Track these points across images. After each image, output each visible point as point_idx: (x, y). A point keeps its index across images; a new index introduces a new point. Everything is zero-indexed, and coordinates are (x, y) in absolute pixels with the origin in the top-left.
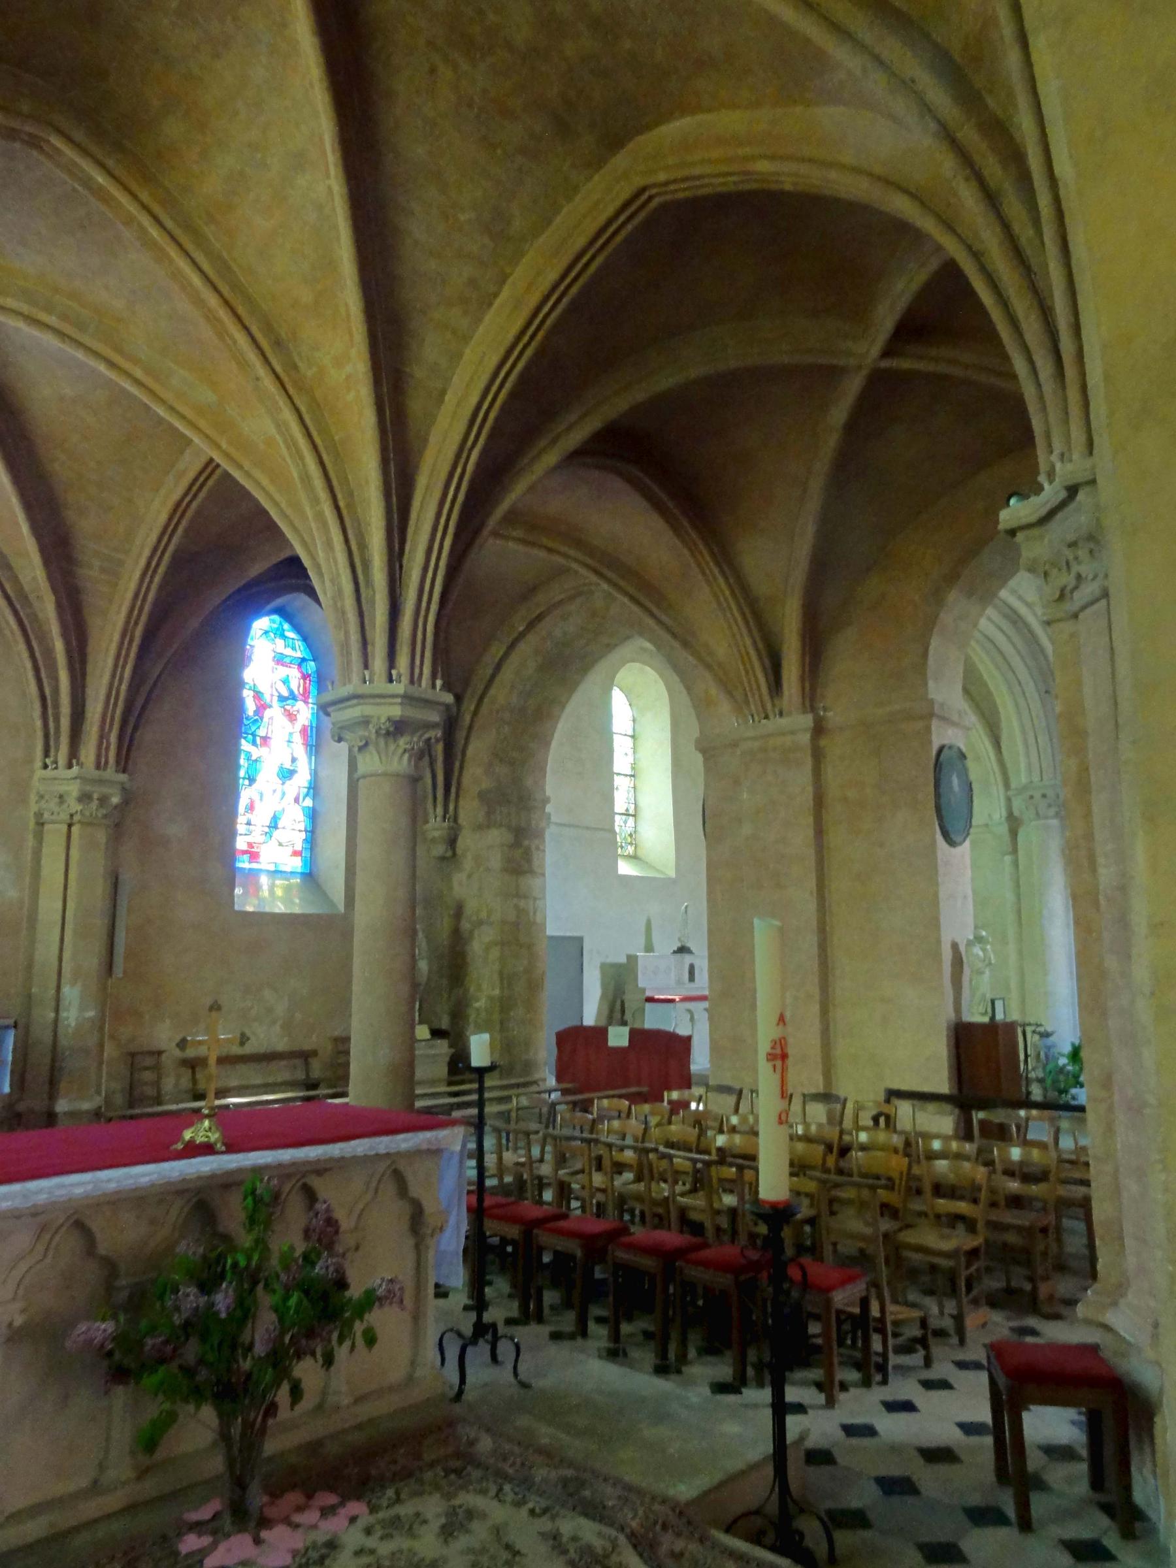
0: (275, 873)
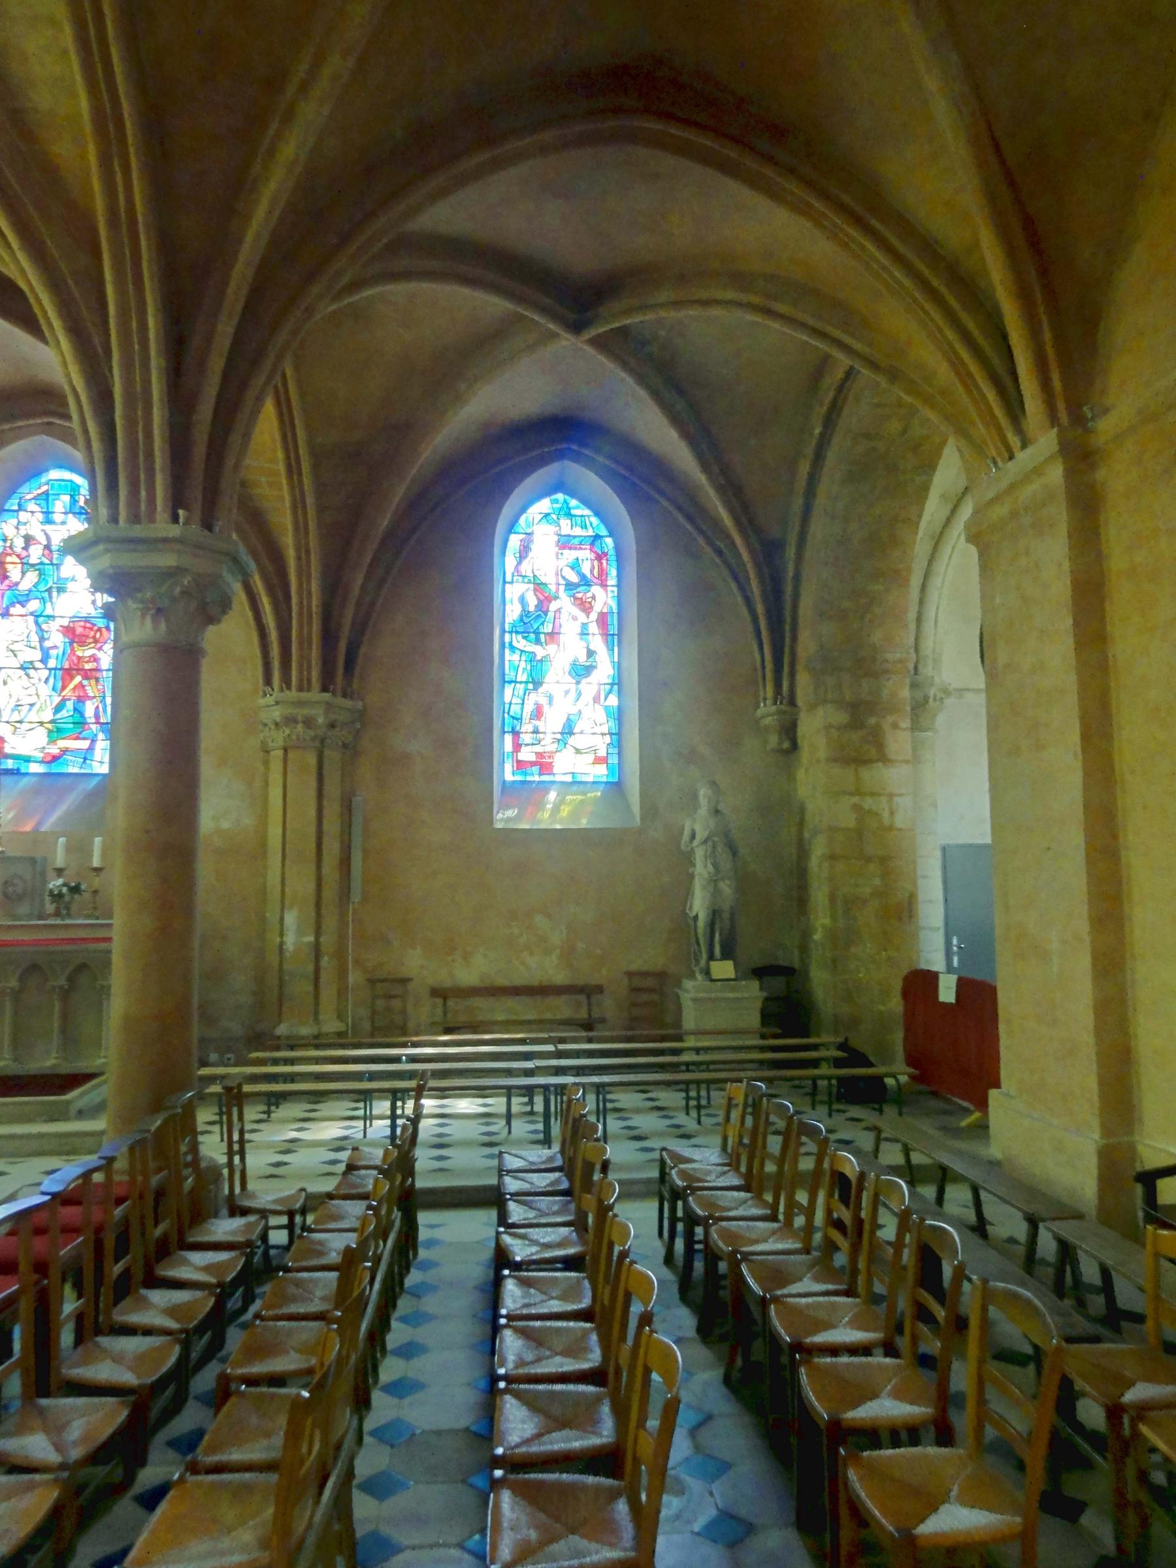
0: (576, 784)
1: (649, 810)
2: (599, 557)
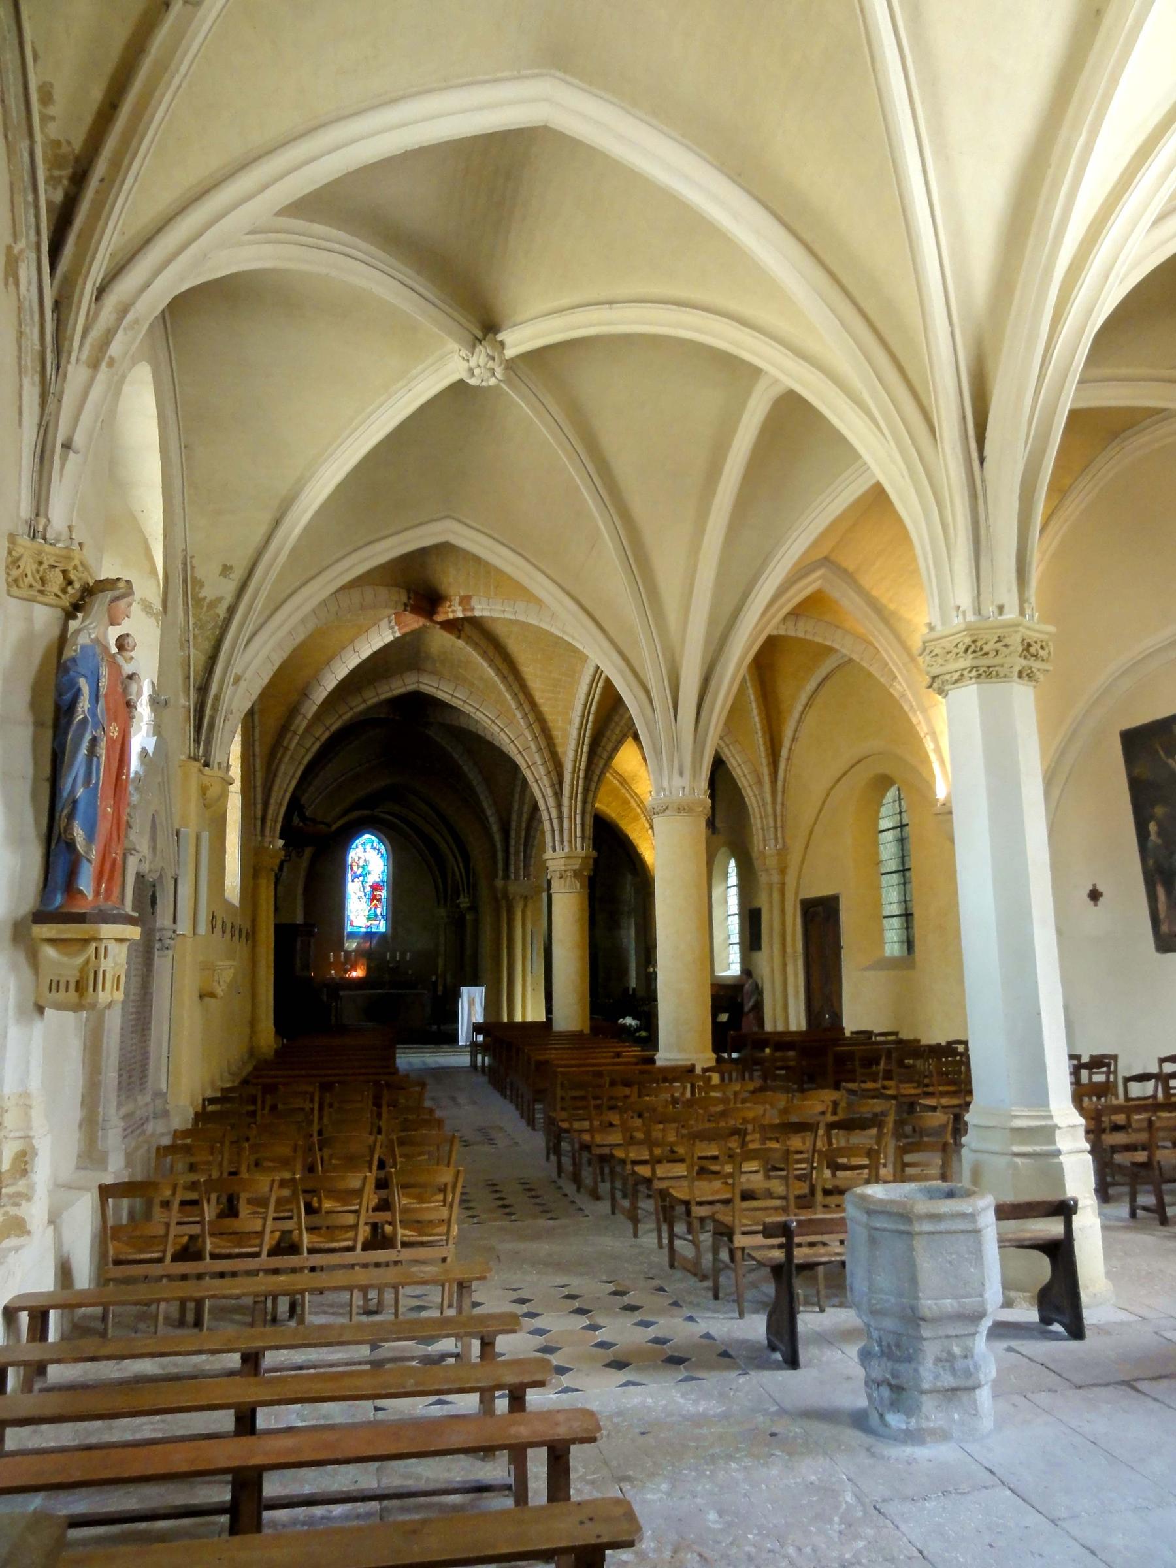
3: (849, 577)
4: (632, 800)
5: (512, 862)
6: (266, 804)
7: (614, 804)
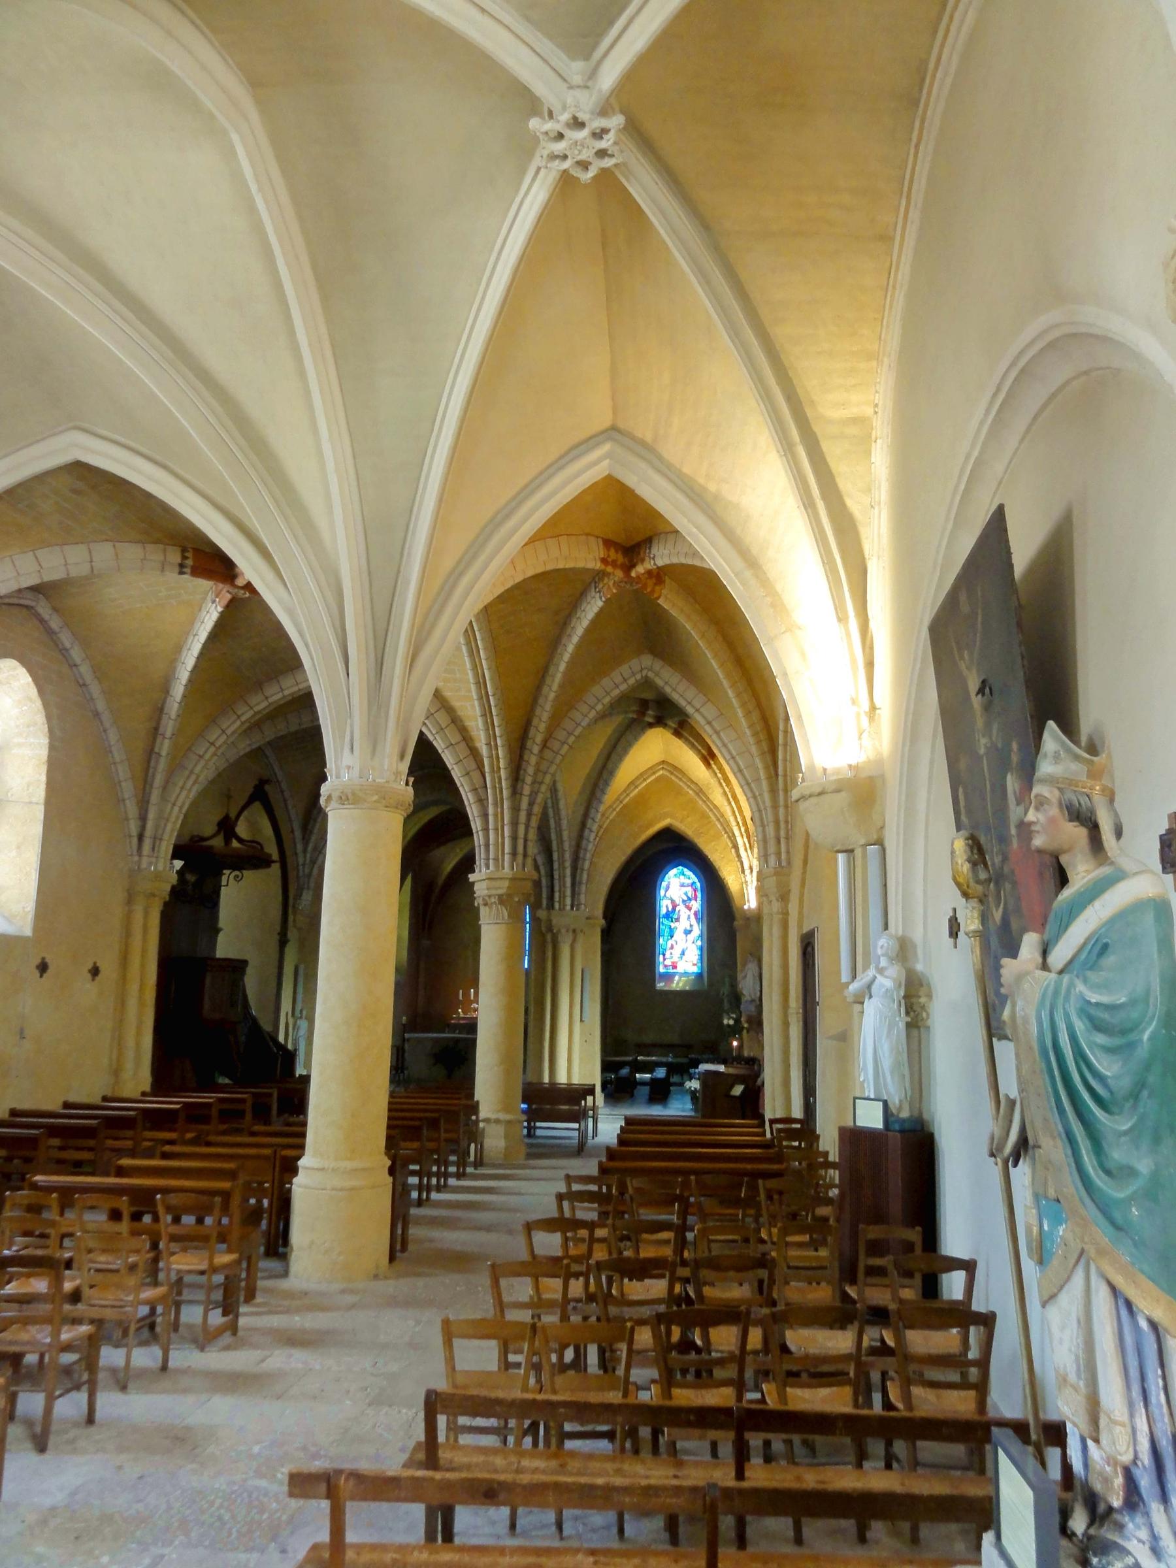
0: (686, 974)
1: (711, 984)
2: (695, 890)
3: (647, 450)
4: (710, 814)
5: (557, 888)
6: (143, 818)
7: (689, 819)
